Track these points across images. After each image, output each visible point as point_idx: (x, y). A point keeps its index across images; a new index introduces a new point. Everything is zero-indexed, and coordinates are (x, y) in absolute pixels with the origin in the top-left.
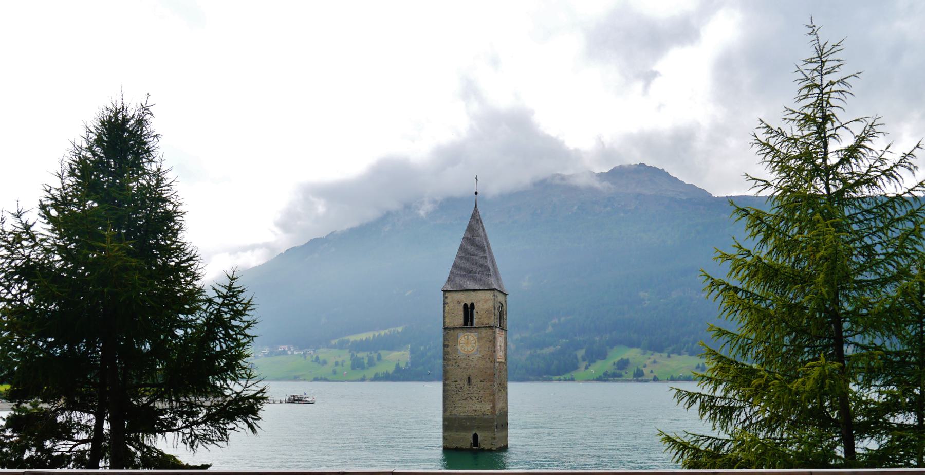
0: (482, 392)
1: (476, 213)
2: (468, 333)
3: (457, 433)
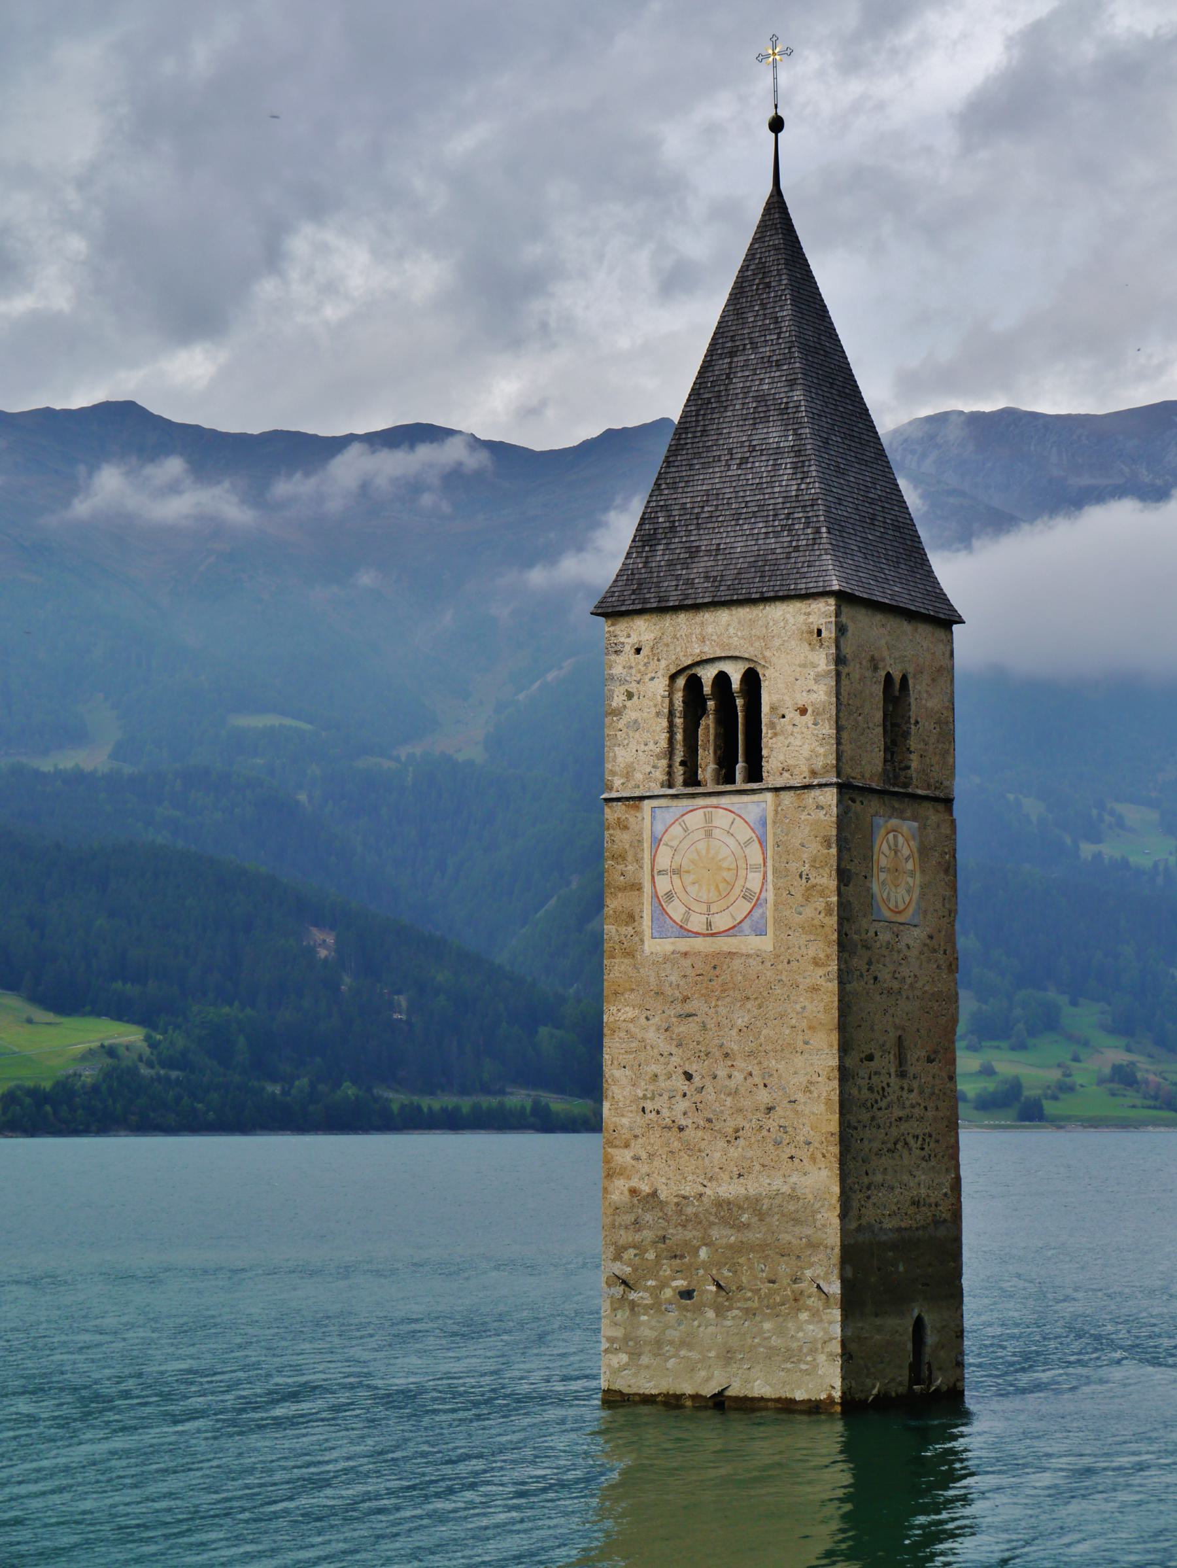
0: (930, 1114)
1: (777, 206)
2: (894, 822)
3: (878, 1321)
